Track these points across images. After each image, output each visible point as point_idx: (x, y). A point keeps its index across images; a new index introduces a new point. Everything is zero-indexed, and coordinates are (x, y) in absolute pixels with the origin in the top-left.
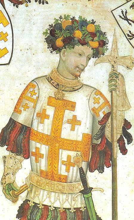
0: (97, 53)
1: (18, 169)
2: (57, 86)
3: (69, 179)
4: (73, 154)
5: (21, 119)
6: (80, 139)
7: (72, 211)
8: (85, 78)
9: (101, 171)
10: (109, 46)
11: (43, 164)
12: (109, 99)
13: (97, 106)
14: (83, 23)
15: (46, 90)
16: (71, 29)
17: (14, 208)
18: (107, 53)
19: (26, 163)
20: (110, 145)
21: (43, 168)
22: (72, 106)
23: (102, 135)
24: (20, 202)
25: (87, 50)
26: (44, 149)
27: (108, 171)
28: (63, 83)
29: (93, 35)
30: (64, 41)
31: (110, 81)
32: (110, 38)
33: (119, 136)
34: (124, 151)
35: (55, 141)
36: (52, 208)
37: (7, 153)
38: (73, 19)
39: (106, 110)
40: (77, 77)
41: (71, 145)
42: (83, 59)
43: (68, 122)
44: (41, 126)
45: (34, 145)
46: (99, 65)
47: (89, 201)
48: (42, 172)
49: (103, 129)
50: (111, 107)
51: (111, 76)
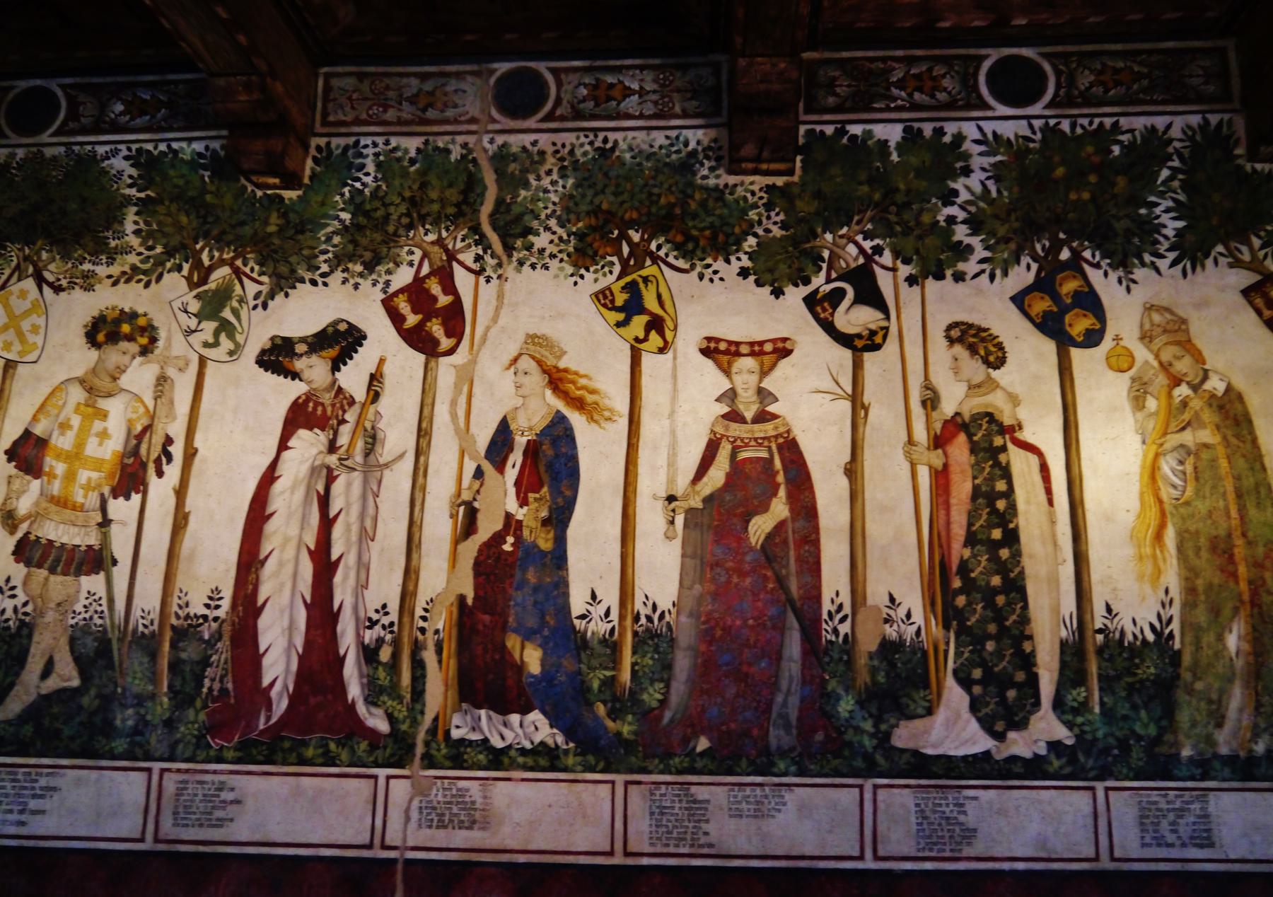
0: (145, 351)
1: (24, 492)
3: (86, 507)
4: (95, 475)
5: (38, 430)
8: (124, 381)
9: (128, 498)
10: (161, 344)
11: (56, 487)
12: (151, 408)
13: (134, 416)
14: (133, 316)
15: (77, 394)
16: (118, 322)
17: (11, 543)
18: (157, 352)
19: (36, 485)
20: (144, 466)
21: (55, 492)
22: (104, 415)
23: (135, 452)
24: (19, 534)
25: (133, 348)
27: (136, 498)
28: (96, 388)
29: (143, 330)
30: (107, 336)
31: (156, 386)
32: (162, 334)
33: (156, 455)
34: (160, 474)
35: (75, 457)
36: (57, 544)
37: (14, 471)
38: (122, 311)
39: (145, 421)
40: (115, 379)
41: (97, 464)
43: (97, 435)
45: (49, 461)
47: (105, 538)
48: (53, 497)
49: (138, 446)
50: (152, 418)
51: (158, 379)
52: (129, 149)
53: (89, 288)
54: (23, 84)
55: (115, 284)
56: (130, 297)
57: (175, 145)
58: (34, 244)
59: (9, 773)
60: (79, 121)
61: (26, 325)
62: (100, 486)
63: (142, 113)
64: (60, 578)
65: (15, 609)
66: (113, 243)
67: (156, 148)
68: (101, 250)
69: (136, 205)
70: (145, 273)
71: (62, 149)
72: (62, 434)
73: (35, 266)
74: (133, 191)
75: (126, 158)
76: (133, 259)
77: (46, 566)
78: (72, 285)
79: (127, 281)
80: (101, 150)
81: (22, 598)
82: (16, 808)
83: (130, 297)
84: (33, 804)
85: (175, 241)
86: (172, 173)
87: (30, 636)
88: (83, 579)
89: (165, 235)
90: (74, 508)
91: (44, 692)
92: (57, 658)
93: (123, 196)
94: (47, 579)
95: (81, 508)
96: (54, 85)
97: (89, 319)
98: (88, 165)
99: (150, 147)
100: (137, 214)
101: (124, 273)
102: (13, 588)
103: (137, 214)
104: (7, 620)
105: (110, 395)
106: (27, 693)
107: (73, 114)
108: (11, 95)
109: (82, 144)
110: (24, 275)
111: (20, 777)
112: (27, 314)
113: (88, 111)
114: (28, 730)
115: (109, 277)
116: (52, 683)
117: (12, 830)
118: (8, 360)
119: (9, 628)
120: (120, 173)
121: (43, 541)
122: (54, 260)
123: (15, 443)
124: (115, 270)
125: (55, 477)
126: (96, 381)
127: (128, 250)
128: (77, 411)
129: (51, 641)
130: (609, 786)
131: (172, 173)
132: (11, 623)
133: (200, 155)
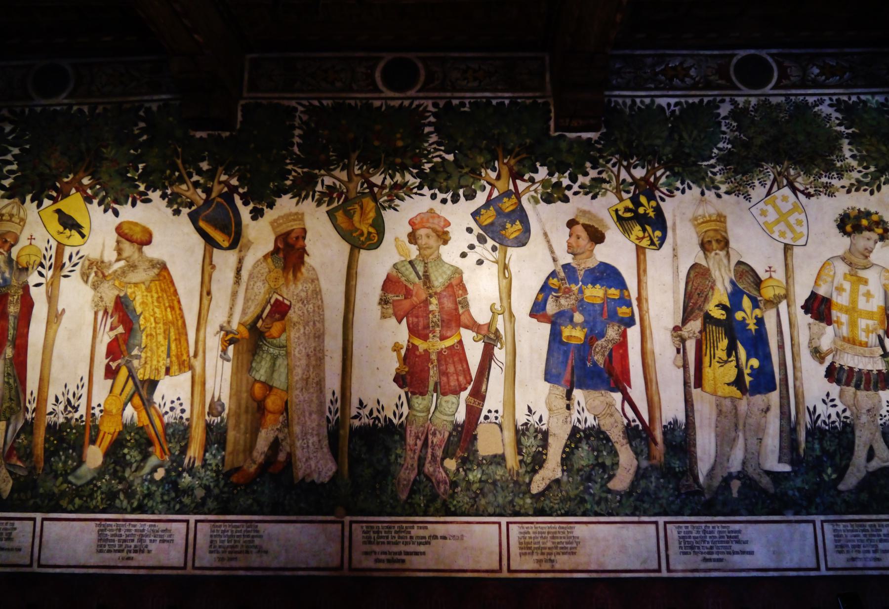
1: (822, 334)
2: (850, 264)
4: (870, 322)
5: (822, 291)
6: (875, 309)
7: (875, 372)
8: (873, 257)
11: (845, 331)
14: (868, 214)
15: (842, 268)
17: (822, 369)
19: (830, 330)
21: (845, 334)
22: (866, 282)
24: (827, 363)
25: (874, 236)
26: (844, 318)
28: (856, 263)
30: (853, 227)
35: (852, 310)
36: (856, 370)
37: (812, 321)
38: (859, 210)
40: (867, 257)
41: (870, 315)
42: (871, 243)
43: (864, 295)
44: (839, 298)
45: (835, 314)
46: (885, 248)
48: (844, 338)
52: (831, 99)
53: (831, 195)
54: (742, 53)
55: (849, 192)
56: (861, 201)
57: (863, 97)
58: (783, 164)
59: (861, 526)
60: (789, 79)
61: (792, 220)
62: (875, 330)
63: (833, 75)
64: (865, 393)
65: (838, 414)
66: (839, 164)
67: (850, 99)
68: (829, 168)
69: (847, 138)
70: (867, 184)
71: (783, 99)
72: (839, 294)
73: (787, 179)
74: (842, 129)
75: (830, 105)
76: (855, 175)
77: (853, 384)
78: (817, 193)
79: (857, 190)
80: (811, 100)
81: (841, 407)
82: (871, 549)
83: (861, 201)
84: (881, 546)
85: (882, 163)
86: (866, 116)
87: (853, 432)
88: (881, 392)
89: (874, 159)
90: (861, 344)
91: (870, 470)
92: (875, 447)
93: (836, 131)
94: (855, 394)
95: (866, 345)
96: (763, 53)
97: (837, 216)
98: (803, 108)
99: (845, 98)
100: (849, 144)
101: (852, 185)
102: (833, 400)
103: (849, 144)
104: (834, 422)
105: (865, 268)
106: (859, 471)
107: (783, 75)
108: (735, 60)
109: (796, 95)
110: (781, 185)
111: (868, 528)
112: (791, 212)
113: (794, 73)
114: (864, 496)
115: (843, 187)
116: (875, 464)
117: (873, 564)
118: (786, 245)
119: (836, 427)
120: (829, 116)
121: (846, 368)
122: (799, 175)
123: (807, 301)
124: (845, 182)
125: (842, 324)
126: (853, 258)
127: (851, 169)
128: (845, 278)
129: (869, 436)
130: (497, 526)
131: (866, 116)
132: (837, 424)
133: (882, 104)
